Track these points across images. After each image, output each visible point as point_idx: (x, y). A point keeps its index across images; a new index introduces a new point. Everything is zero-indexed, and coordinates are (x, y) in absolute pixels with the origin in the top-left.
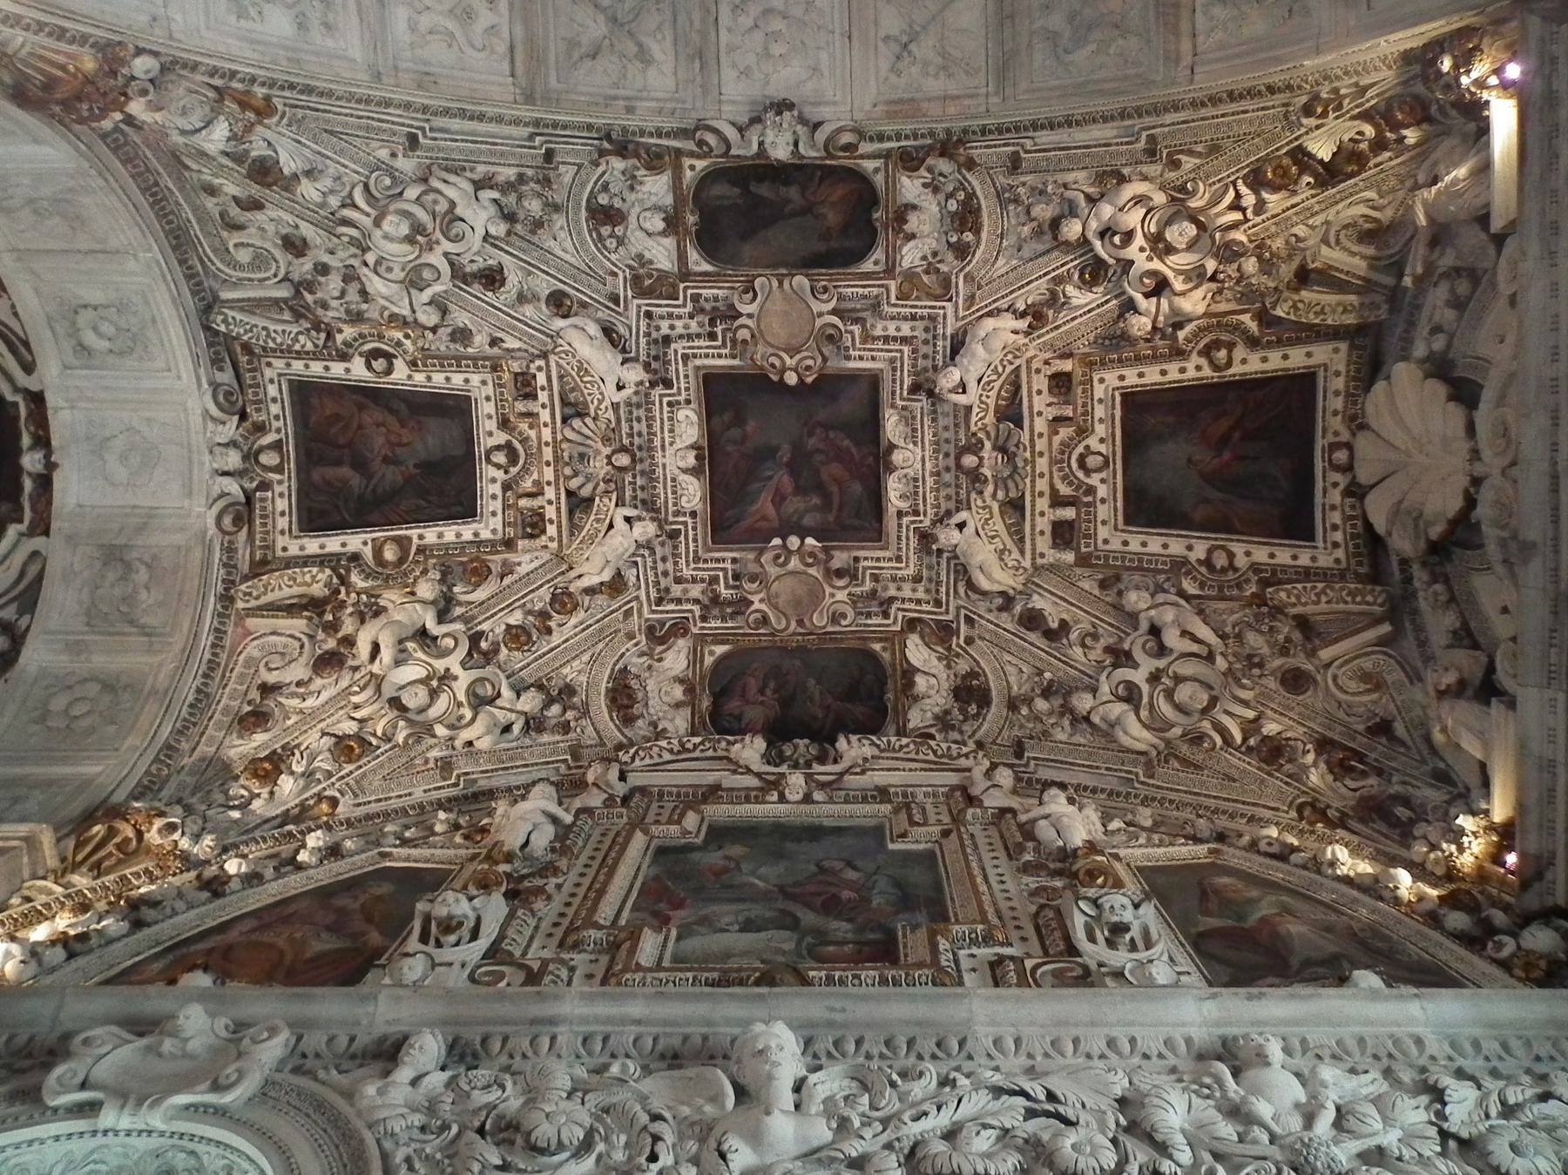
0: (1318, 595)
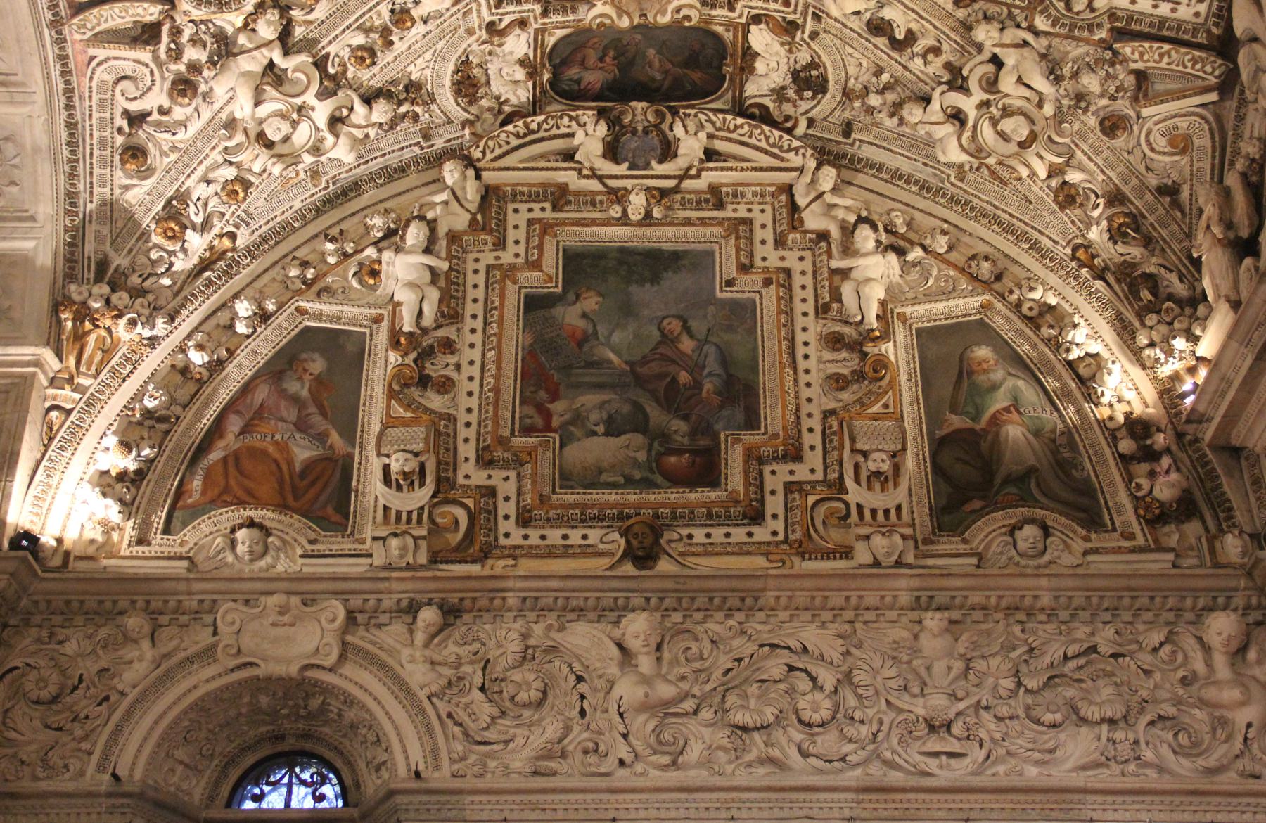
0: (1161, 56)
